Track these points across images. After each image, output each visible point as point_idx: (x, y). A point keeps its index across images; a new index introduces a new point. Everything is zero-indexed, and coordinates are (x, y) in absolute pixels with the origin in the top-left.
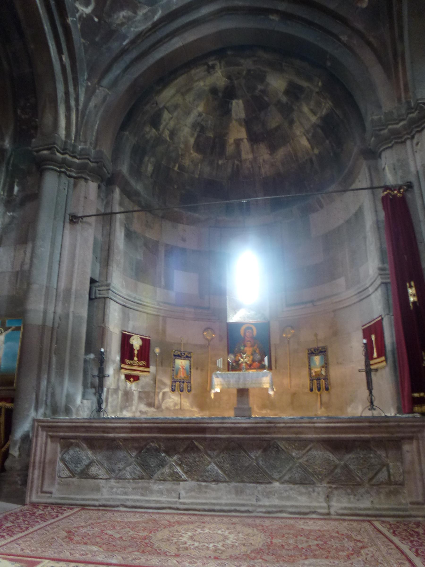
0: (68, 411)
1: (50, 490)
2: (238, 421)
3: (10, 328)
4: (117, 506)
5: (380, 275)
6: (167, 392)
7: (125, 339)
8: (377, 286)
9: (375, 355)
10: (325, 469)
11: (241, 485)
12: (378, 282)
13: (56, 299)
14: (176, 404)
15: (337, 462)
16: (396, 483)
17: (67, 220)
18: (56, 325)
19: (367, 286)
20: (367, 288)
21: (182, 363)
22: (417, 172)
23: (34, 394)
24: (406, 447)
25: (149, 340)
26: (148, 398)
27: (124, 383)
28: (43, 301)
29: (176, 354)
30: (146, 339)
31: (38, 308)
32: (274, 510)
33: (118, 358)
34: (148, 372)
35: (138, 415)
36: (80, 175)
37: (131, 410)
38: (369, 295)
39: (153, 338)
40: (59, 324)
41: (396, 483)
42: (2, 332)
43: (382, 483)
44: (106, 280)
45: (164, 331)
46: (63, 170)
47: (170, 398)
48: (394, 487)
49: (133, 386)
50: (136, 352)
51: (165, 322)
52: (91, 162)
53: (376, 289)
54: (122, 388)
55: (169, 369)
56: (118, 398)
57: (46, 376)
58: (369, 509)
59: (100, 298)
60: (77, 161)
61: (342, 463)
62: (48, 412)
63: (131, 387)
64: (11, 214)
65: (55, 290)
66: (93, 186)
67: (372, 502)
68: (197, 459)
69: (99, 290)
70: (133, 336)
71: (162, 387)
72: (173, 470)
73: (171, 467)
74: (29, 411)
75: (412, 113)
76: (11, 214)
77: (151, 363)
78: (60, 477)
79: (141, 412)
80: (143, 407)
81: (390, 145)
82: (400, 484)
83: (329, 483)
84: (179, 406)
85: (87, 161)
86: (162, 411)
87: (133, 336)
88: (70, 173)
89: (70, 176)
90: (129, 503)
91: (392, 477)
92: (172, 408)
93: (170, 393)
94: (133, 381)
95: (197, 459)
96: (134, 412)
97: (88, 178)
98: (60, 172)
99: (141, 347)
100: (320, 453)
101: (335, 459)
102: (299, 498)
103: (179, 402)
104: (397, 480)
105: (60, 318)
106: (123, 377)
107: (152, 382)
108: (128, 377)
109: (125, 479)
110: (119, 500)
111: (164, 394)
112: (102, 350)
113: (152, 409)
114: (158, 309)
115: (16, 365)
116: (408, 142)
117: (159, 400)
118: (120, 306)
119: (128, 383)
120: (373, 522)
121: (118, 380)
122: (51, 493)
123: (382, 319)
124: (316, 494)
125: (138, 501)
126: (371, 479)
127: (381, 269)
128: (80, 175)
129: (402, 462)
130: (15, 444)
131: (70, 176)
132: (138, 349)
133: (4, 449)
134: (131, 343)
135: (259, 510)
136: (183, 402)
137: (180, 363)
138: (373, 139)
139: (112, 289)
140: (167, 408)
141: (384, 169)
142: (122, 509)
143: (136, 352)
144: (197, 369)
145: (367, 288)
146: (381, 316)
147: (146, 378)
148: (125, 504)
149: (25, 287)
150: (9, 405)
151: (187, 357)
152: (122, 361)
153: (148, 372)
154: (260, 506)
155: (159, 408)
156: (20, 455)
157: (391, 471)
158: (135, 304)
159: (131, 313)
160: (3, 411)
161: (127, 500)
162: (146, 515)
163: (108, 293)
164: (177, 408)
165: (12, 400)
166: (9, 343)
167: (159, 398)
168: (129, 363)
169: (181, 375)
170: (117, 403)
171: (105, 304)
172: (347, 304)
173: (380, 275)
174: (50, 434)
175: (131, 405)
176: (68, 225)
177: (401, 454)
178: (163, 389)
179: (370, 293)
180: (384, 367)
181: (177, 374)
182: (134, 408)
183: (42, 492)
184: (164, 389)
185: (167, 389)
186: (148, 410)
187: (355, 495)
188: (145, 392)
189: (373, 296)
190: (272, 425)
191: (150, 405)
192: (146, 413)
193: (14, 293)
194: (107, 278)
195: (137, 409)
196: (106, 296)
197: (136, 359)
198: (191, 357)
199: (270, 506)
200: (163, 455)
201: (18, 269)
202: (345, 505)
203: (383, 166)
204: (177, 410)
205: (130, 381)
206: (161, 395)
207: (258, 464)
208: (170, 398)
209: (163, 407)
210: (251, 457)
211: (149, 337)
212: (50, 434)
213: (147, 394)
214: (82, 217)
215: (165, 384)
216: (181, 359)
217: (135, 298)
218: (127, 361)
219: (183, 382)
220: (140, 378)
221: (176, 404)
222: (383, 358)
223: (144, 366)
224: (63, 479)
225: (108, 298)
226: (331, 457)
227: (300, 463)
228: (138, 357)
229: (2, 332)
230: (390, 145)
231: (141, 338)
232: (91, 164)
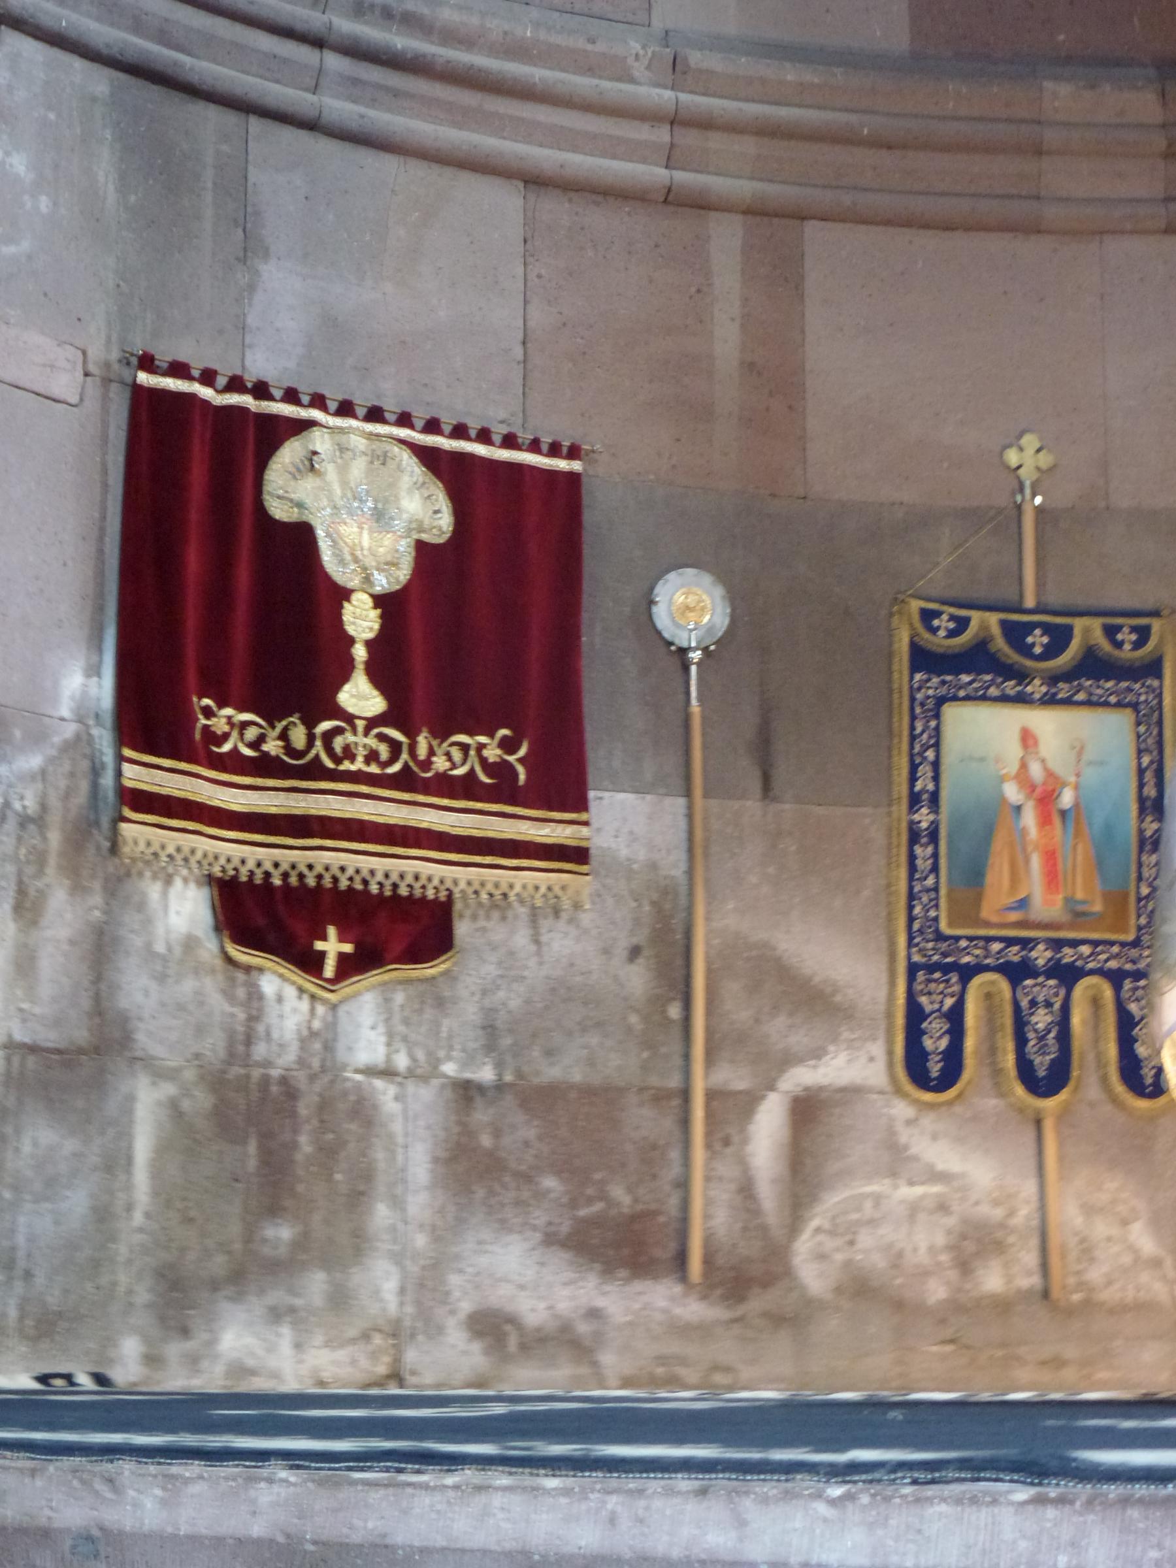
6: (851, 1093)
14: (976, 1243)
21: (1027, 738)
27: (208, 992)
29: (940, 641)
33: (83, 685)
34: (577, 855)
37: (340, 1299)
39: (622, 464)
45: (777, 379)
47: (896, 1160)
49: (368, 1023)
50: (361, 620)
51: (778, 272)
54: (157, 1034)
55: (878, 826)
56: (116, 1163)
63: (323, 1041)
70: (302, 426)
71: (781, 1031)
77: (602, 753)
79: (491, 1327)
80: (517, 1271)
84: (1029, 1258)
86: (795, 1319)
87: (310, 424)
93: (901, 1110)
94: (349, 967)
96: (396, 1332)
103: (1025, 1213)
106: (185, 910)
107: (637, 979)
108: (260, 917)
111: (807, 1110)
113: (660, 1297)
114: (676, 120)
117: (746, 1190)
118: (101, 81)
119: (277, 982)
121: (101, 949)
132: (396, 575)
134: (279, 511)
136: (1068, 1214)
137: (1014, 751)
140: (859, 1288)
143: (361, 620)
147: (540, 939)
151: (1093, 666)
152: (149, 714)
153: (577, 855)
155: (746, 1278)
158: (334, 62)
159: (282, 172)
164: (992, 1280)
167: (743, 1163)
168: (272, 747)
169: (1031, 887)
170: (103, 1216)
175: (345, 1248)
178: (788, 1060)
181: (974, 876)
182: (383, 1284)
184: (818, 1054)
185: (858, 1064)
186: (594, 1314)
188: (541, 1099)
191: (630, 1244)
192: (567, 1341)
195: (426, 1286)
197: (360, 696)
198: (1154, 668)
204: (1002, 1306)
205: (311, 963)
206: (768, 1126)
208: (896, 1160)
209: (812, 1266)
211: (574, 453)
213: (577, 1121)
215: (816, 1003)
216: (1021, 699)
218: (229, 722)
219: (1068, 975)
220: (462, 929)
221: (976, 1243)
223: (501, 789)
228: (378, 676)
231: (428, 457)
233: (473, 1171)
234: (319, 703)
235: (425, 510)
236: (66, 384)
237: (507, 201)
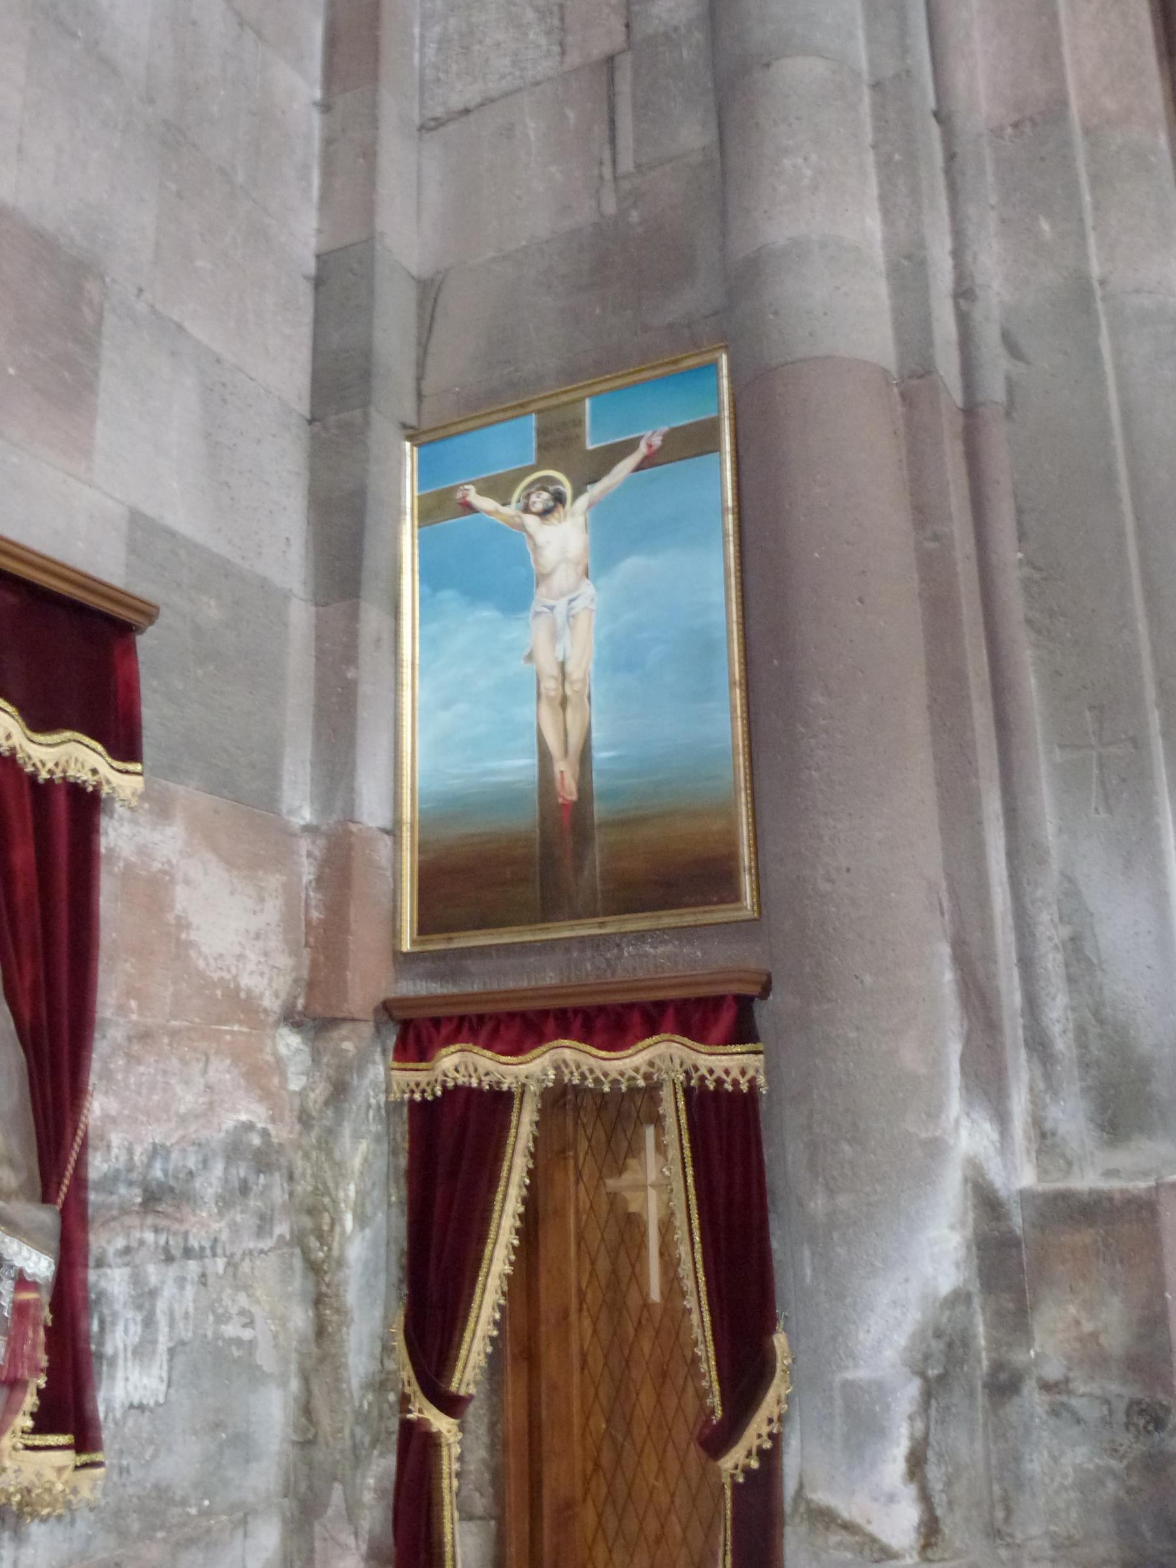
3: (629, 447)
18: (994, 389)
23: (945, 950)
28: (873, 189)
40: (1011, 386)
42: (559, 498)
62: (1071, 1117)
74: (934, 1112)
105: (1007, 339)
115: (721, 722)
130: (862, 1423)
133: (736, 1459)
149: (692, 135)
150: (726, 1064)
156: (930, 1531)
160: (672, 1107)
165: (726, 1015)
166: (631, 564)
193: (610, 206)
201: (606, 36)
229: (559, 498)
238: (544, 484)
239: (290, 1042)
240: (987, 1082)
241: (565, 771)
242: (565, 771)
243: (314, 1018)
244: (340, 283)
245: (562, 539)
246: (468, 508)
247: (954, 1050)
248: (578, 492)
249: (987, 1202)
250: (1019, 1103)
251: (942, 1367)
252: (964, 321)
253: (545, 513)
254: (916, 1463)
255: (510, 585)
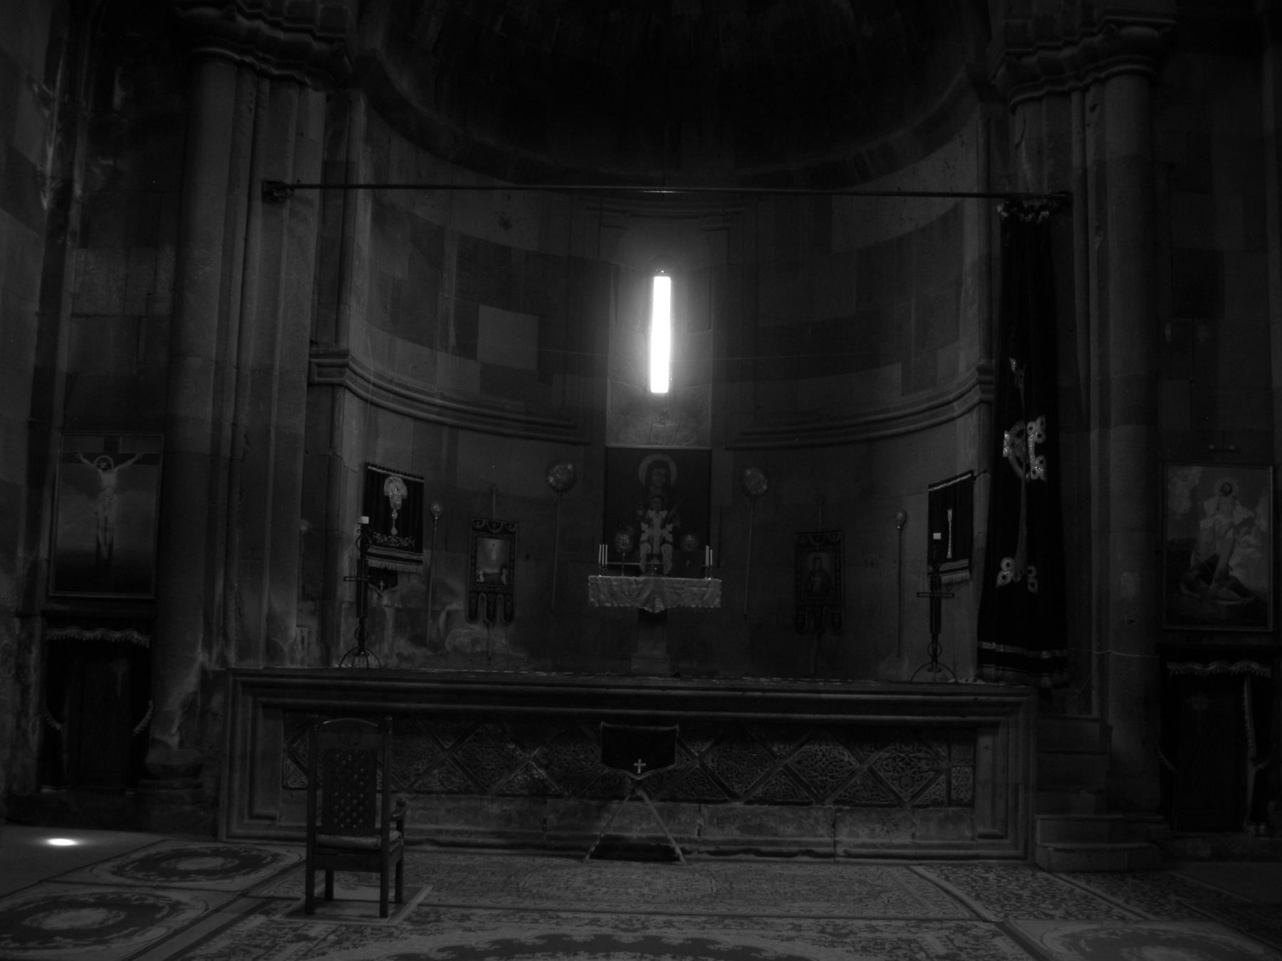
0: (272, 650)
1: (271, 811)
2: (669, 684)
3: (132, 456)
4: (419, 843)
5: (980, 382)
6: (456, 611)
7: (373, 481)
8: (970, 404)
9: (949, 554)
10: (832, 777)
11: (670, 804)
12: (975, 397)
13: (237, 394)
14: (475, 642)
15: (856, 765)
16: (959, 803)
17: (258, 192)
19: (951, 397)
20: (950, 402)
22: (1085, 170)
24: (985, 741)
25: (422, 484)
26: (412, 622)
30: (416, 483)
31: (199, 409)
32: (734, 848)
35: (393, 662)
36: (286, 72)
38: (953, 419)
41: (959, 803)
43: (936, 803)
44: (337, 341)
46: (248, 59)
48: (954, 809)
50: (395, 515)
52: (316, 38)
53: (969, 410)
57: (222, 573)
58: (905, 846)
59: (319, 384)
60: (282, 36)
61: (865, 767)
64: (111, 162)
65: (234, 371)
66: (316, 100)
67: (913, 836)
68: (582, 757)
69: (319, 365)
70: (388, 476)
72: (531, 776)
73: (528, 769)
75: (1093, 35)
76: (111, 162)
78: (286, 787)
79: (399, 655)
80: (404, 646)
81: (1036, 94)
82: (966, 805)
83: (836, 802)
85: (307, 38)
88: (264, 66)
89: (263, 74)
90: (443, 838)
91: (953, 793)
92: (468, 651)
95: (582, 757)
97: (307, 80)
98: (241, 65)
99: (405, 501)
100: (824, 748)
101: (852, 759)
102: (781, 829)
104: (962, 796)
109: (429, 793)
110: (421, 832)
111: (449, 614)
112: (366, 520)
116: (1075, 97)
120: (915, 868)
122: (272, 818)
123: (973, 478)
124: (812, 821)
125: (461, 832)
126: (914, 796)
127: (982, 370)
128: (286, 72)
129: (974, 767)
131: (263, 74)
135: (703, 848)
138: (1002, 70)
139: (351, 364)
141: (1018, 145)
142: (428, 847)
143: (395, 515)
144: (527, 557)
145: (950, 402)
146: (971, 472)
148: (436, 838)
154: (705, 843)
156: (181, 743)
157: (954, 781)
161: (440, 832)
162: (477, 857)
163: (342, 375)
171: (334, 400)
172: (902, 429)
173: (980, 382)
174: (264, 699)
176: (258, 205)
177: (975, 751)
179: (955, 414)
180: (964, 581)
182: (386, 647)
183: (252, 817)
185: (458, 605)
187: (884, 824)
189: (960, 421)
190: (739, 693)
191: (418, 640)
192: (410, 659)
194: (337, 334)
196: (336, 380)
197: (394, 531)
199: (725, 843)
200: (512, 746)
202: (864, 839)
203: (1017, 140)
207: (703, 765)
210: (691, 754)
212: (264, 699)
214: (293, 187)
217: (391, 381)
221: (475, 642)
222: (965, 562)
224: (294, 793)
225: (341, 385)
226: (847, 757)
227: (786, 766)
230: (1036, 94)
231: (405, 481)
232: (317, 46)
233: (398, 625)
234: (388, 533)
235: (404, 491)
236: (356, 469)
237: (410, 422)
238: (105, 460)
239: (17, 621)
240: (208, 646)
241: (104, 550)
242: (104, 550)
243: (24, 616)
244: (43, 379)
245: (109, 479)
246: (80, 461)
247: (201, 636)
248: (116, 465)
249: (204, 672)
250: (215, 650)
251: (189, 707)
252: (234, 433)
253: (105, 470)
254: (180, 728)
255: (93, 490)
